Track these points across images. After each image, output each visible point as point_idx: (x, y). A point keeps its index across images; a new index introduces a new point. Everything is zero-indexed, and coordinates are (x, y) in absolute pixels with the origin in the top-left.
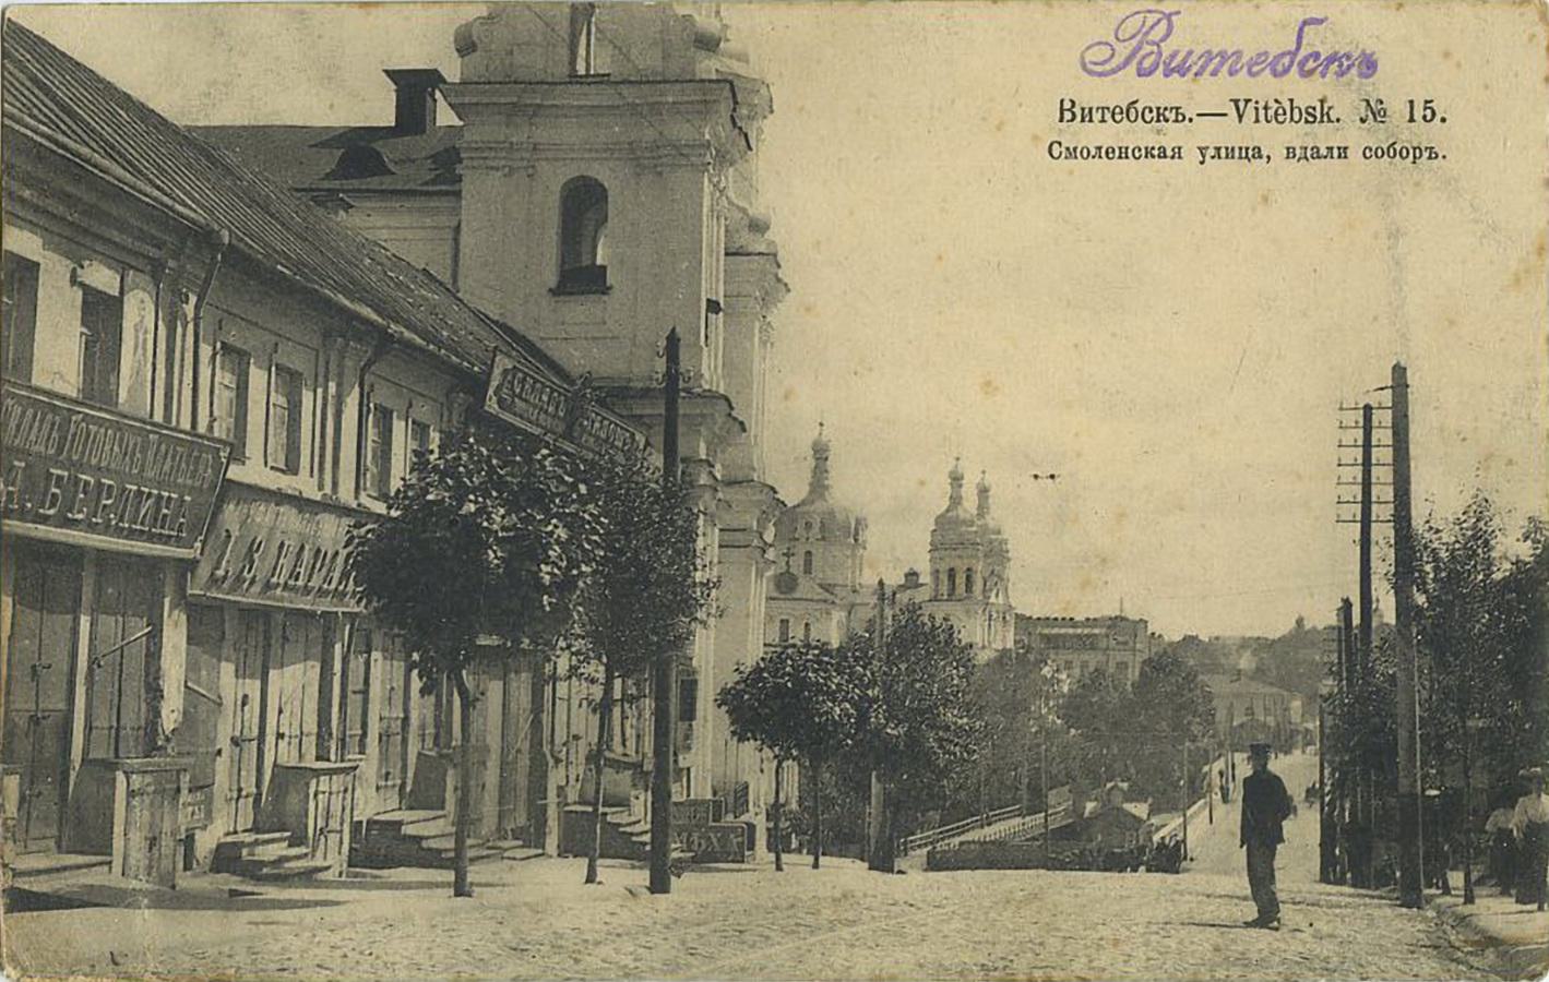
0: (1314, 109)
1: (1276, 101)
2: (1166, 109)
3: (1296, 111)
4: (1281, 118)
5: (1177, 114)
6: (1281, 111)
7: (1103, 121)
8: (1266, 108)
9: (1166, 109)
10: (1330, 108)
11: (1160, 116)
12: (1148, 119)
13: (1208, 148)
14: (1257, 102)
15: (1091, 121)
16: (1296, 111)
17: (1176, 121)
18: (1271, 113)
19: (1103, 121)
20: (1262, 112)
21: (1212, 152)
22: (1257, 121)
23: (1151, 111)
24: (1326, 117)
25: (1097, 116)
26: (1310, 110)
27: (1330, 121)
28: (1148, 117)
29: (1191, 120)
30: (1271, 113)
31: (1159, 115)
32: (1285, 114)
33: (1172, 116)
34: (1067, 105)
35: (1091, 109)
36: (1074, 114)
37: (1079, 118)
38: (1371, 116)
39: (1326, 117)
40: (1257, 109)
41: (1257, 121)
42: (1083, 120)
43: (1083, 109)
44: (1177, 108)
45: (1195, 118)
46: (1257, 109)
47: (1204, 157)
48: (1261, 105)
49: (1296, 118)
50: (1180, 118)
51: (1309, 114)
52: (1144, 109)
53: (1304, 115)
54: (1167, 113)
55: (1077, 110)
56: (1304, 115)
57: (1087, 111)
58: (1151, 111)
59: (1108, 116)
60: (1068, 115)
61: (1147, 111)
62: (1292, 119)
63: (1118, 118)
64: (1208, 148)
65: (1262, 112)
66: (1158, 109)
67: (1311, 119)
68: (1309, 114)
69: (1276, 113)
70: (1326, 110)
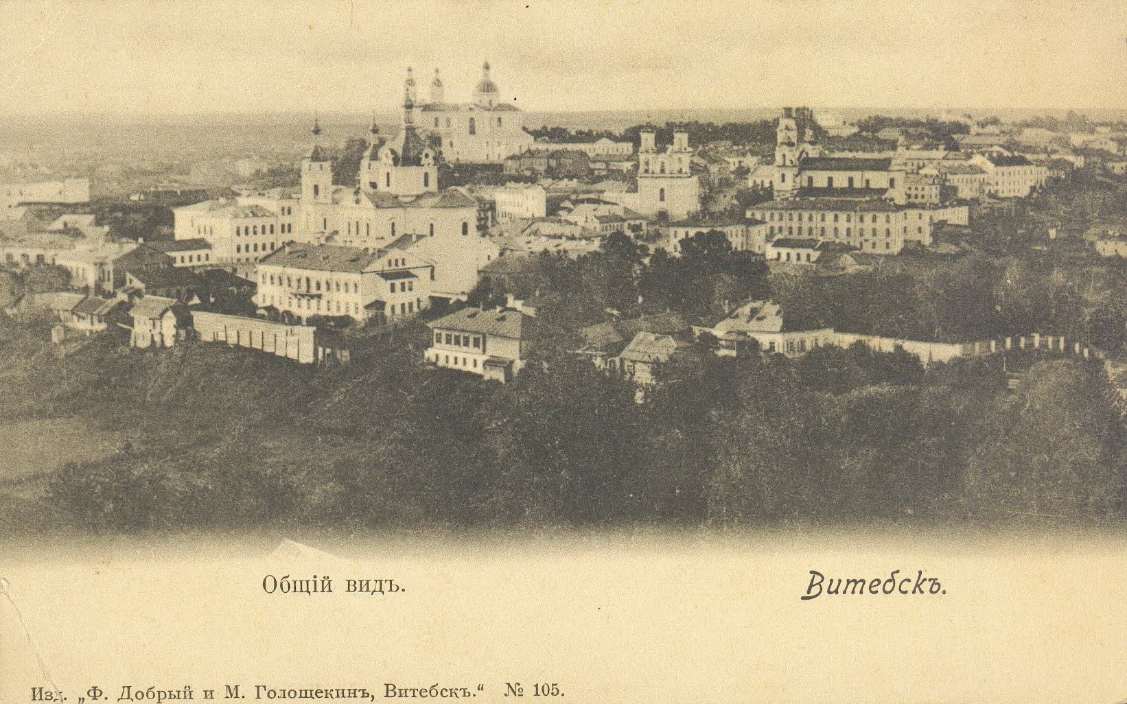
5: (465, 692)
7: (414, 696)
15: (406, 696)
19: (414, 696)
25: (410, 694)
28: (445, 693)
31: (451, 693)
33: (460, 694)
34: (391, 687)
36: (395, 693)
37: (398, 694)
42: (400, 696)
44: (464, 690)
54: (457, 692)
55: (396, 690)
57: (403, 691)
59: (417, 693)
60: (391, 693)
61: (444, 691)
63: (424, 694)
66: (451, 690)
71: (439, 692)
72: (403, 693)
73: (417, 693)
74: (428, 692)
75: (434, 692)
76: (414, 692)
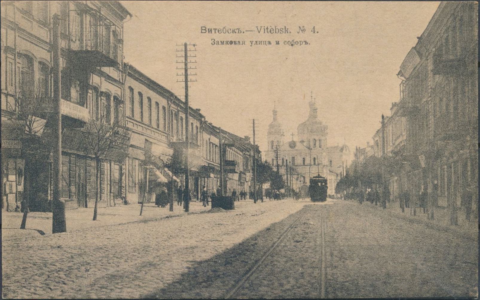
0: (283, 29)
1: (271, 27)
2: (235, 30)
3: (277, 30)
4: (272, 32)
6: (272, 30)
8: (267, 28)
9: (235, 30)
10: (288, 29)
11: (234, 31)
12: (230, 32)
13: (253, 41)
14: (264, 27)
15: (211, 33)
16: (277, 29)
17: (239, 33)
18: (269, 30)
19: (215, 32)
20: (266, 30)
21: (254, 43)
22: (264, 33)
23: (230, 30)
24: (286, 31)
25: (213, 31)
26: (282, 30)
27: (288, 32)
28: (230, 31)
29: (243, 32)
30: (269, 30)
31: (233, 31)
32: (273, 30)
33: (237, 31)
35: (211, 29)
38: (301, 31)
39: (286, 31)
40: (264, 29)
41: (264, 33)
43: (209, 29)
44: (239, 29)
45: (245, 32)
46: (264, 29)
47: (252, 44)
48: (266, 28)
49: (277, 32)
50: (240, 32)
51: (281, 31)
52: (228, 30)
53: (280, 31)
56: (280, 31)
57: (210, 30)
58: (230, 30)
59: (217, 31)
62: (276, 32)
63: (220, 32)
64: (253, 41)
65: (266, 30)
67: (282, 32)
68: (281, 31)
69: (270, 31)
70: (286, 30)
71: (227, 32)
72: (210, 31)
73: (217, 31)
74: (222, 31)
75: (224, 30)
76: (215, 30)
